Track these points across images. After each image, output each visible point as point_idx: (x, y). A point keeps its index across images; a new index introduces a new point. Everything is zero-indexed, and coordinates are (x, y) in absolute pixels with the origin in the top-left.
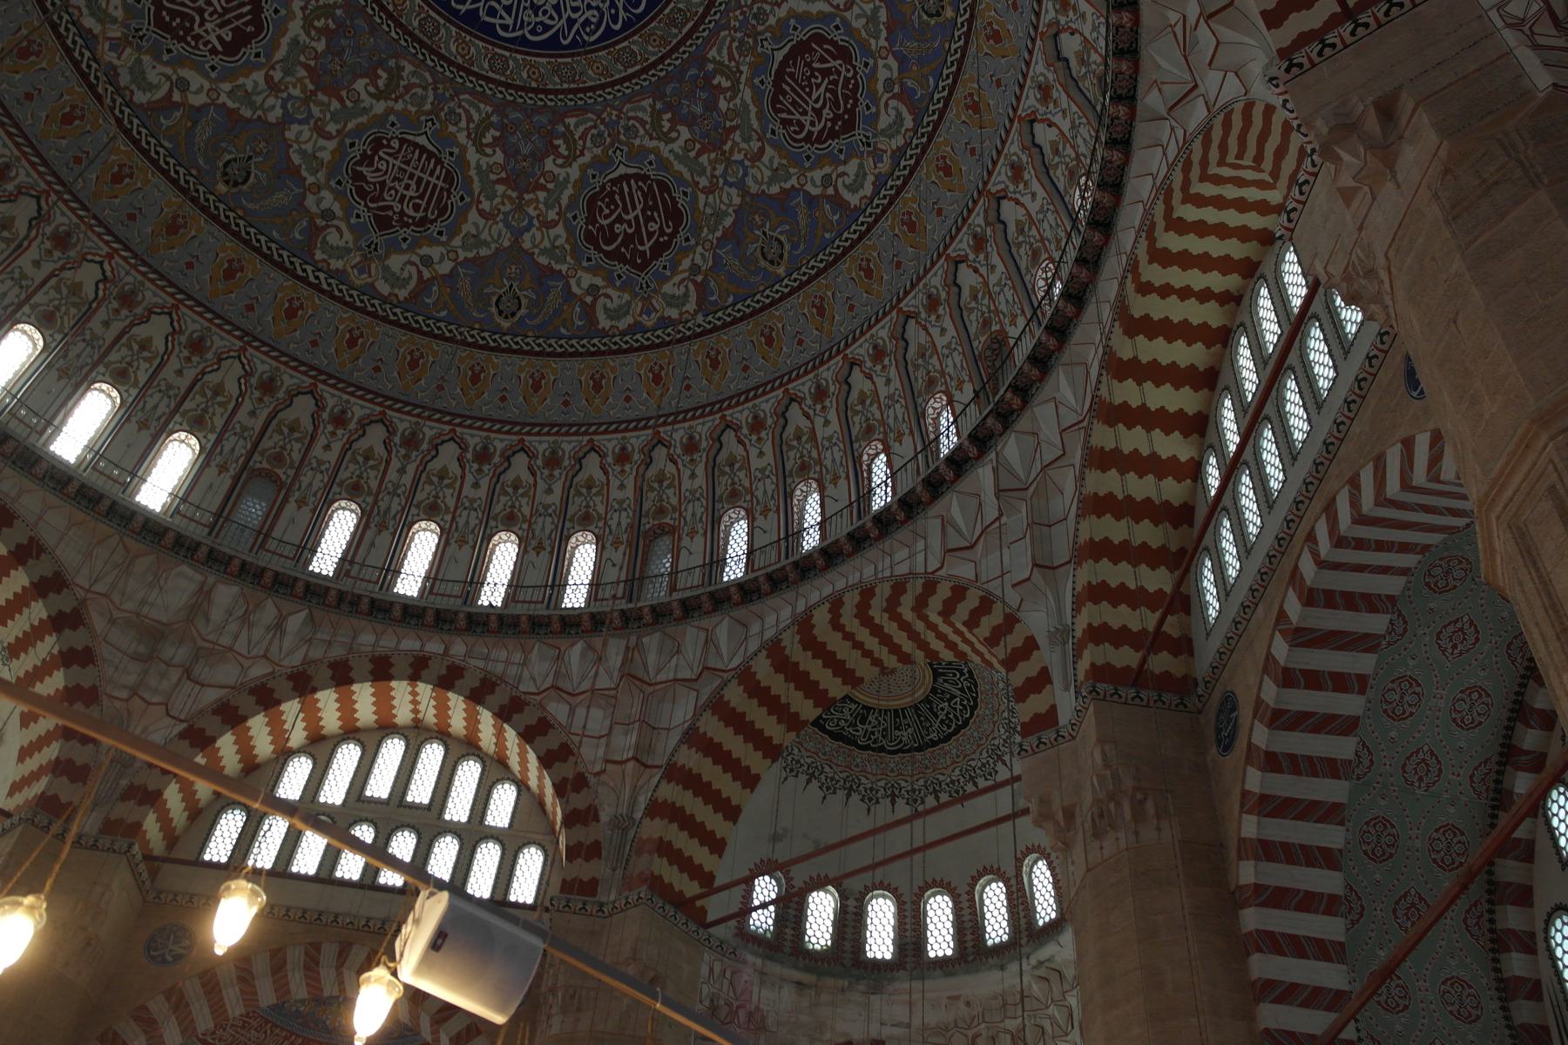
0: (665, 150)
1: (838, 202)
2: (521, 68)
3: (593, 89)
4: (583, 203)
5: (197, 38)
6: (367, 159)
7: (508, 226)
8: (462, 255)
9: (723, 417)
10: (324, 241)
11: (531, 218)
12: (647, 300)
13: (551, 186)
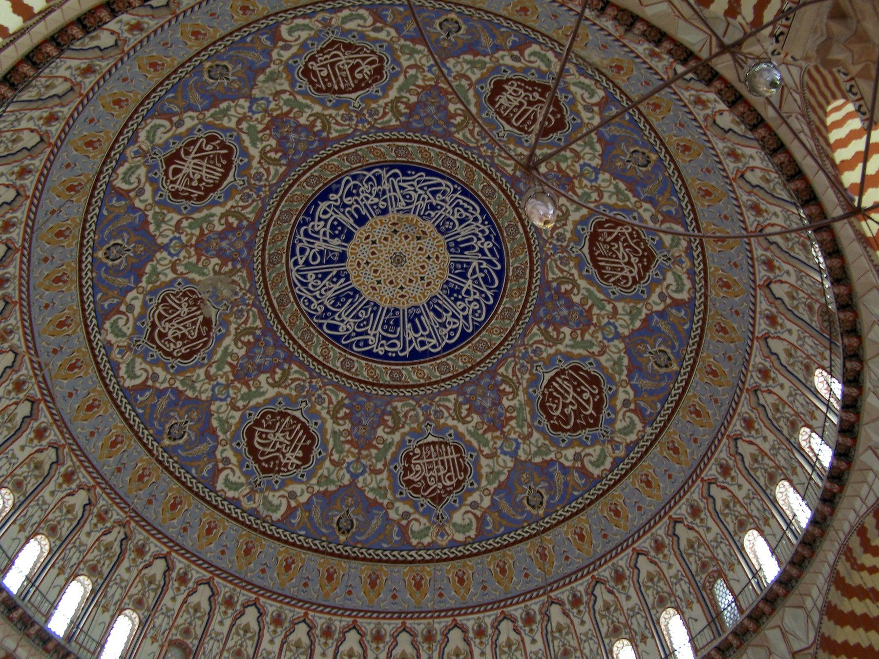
2: (456, 361)
3: (501, 344)
5: (286, 465)
6: (407, 470)
7: (505, 454)
8: (492, 488)
9: (702, 480)
10: (412, 532)
11: (516, 440)
12: (611, 441)
13: (515, 414)
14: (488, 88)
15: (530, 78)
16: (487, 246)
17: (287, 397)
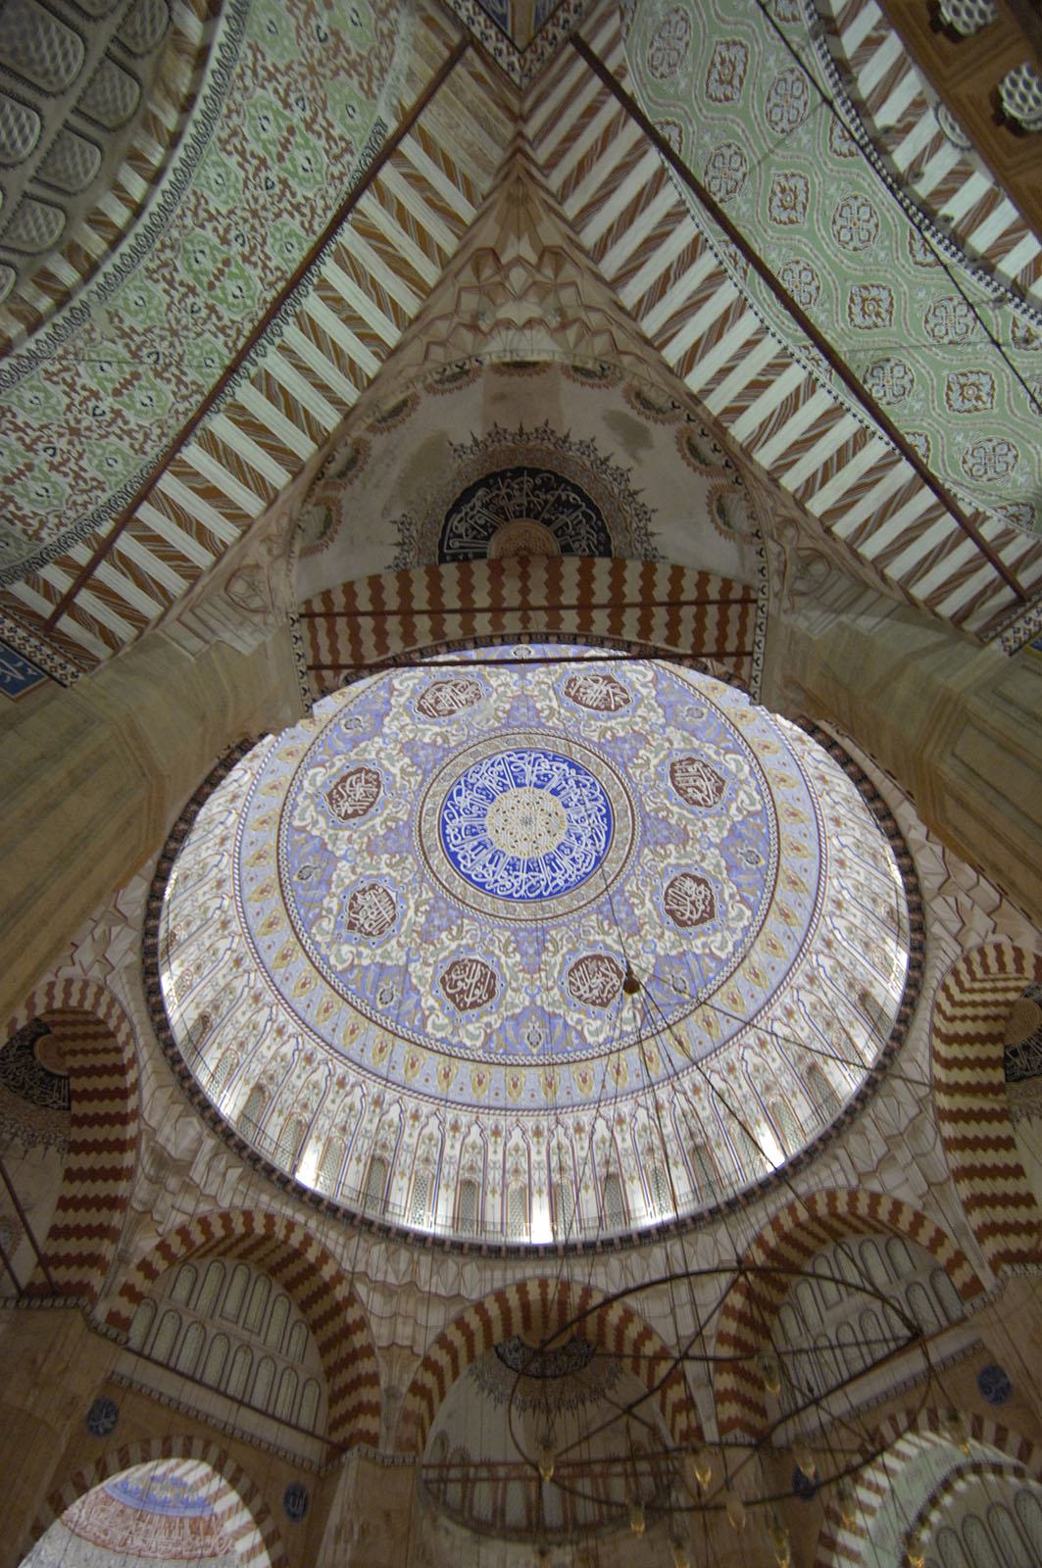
0: (503, 959)
1: (580, 1034)
2: (459, 885)
6: (364, 892)
14: (698, 874)
15: (717, 904)
16: (561, 883)
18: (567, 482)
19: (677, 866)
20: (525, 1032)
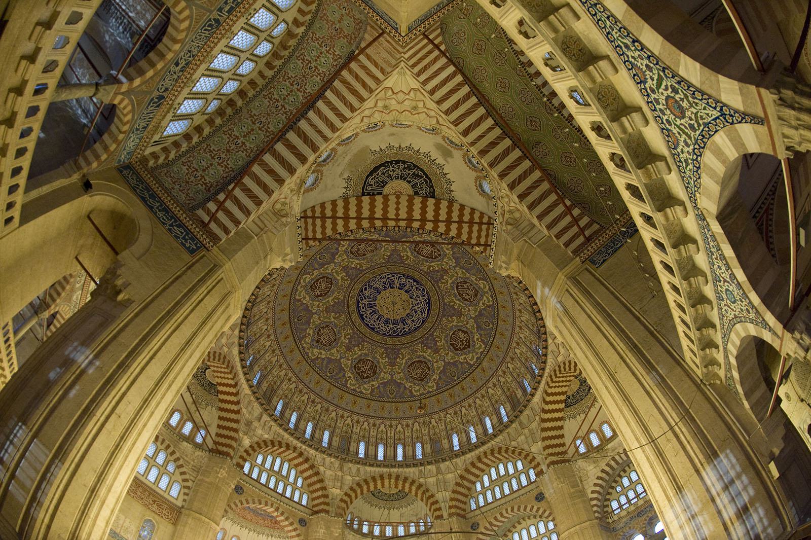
0: (381, 360)
1: (411, 391)
2: (364, 329)
4: (357, 360)
6: (323, 328)
14: (465, 329)
17: (338, 283)
18: (418, 167)
19: (456, 326)
20: (388, 389)
